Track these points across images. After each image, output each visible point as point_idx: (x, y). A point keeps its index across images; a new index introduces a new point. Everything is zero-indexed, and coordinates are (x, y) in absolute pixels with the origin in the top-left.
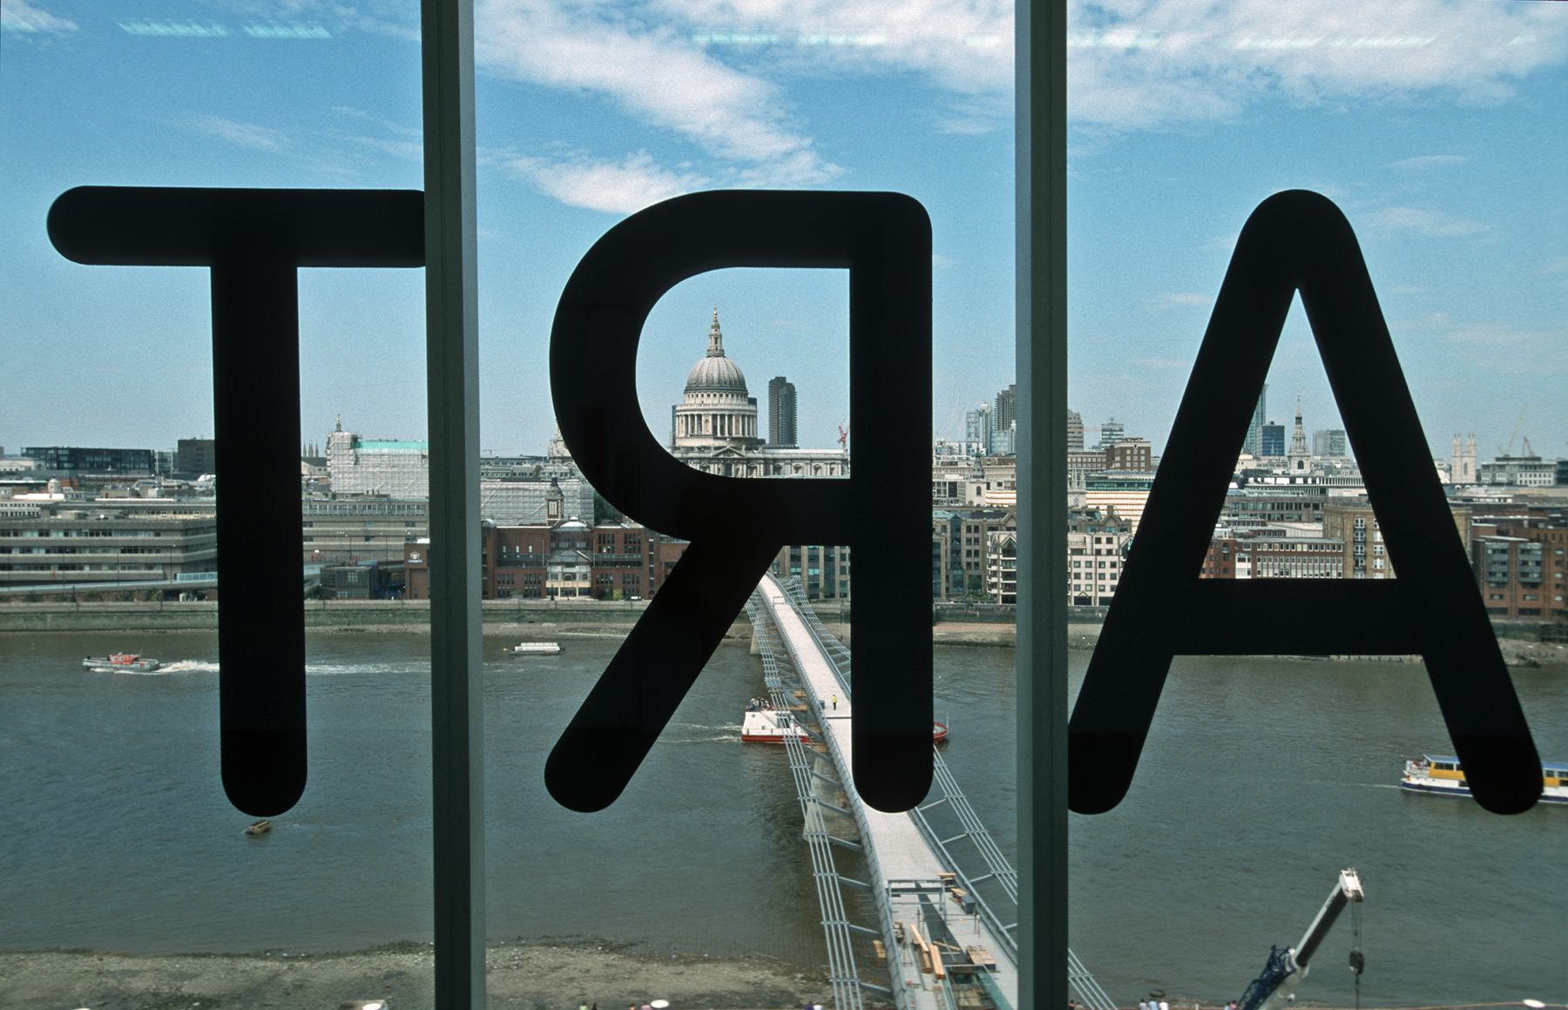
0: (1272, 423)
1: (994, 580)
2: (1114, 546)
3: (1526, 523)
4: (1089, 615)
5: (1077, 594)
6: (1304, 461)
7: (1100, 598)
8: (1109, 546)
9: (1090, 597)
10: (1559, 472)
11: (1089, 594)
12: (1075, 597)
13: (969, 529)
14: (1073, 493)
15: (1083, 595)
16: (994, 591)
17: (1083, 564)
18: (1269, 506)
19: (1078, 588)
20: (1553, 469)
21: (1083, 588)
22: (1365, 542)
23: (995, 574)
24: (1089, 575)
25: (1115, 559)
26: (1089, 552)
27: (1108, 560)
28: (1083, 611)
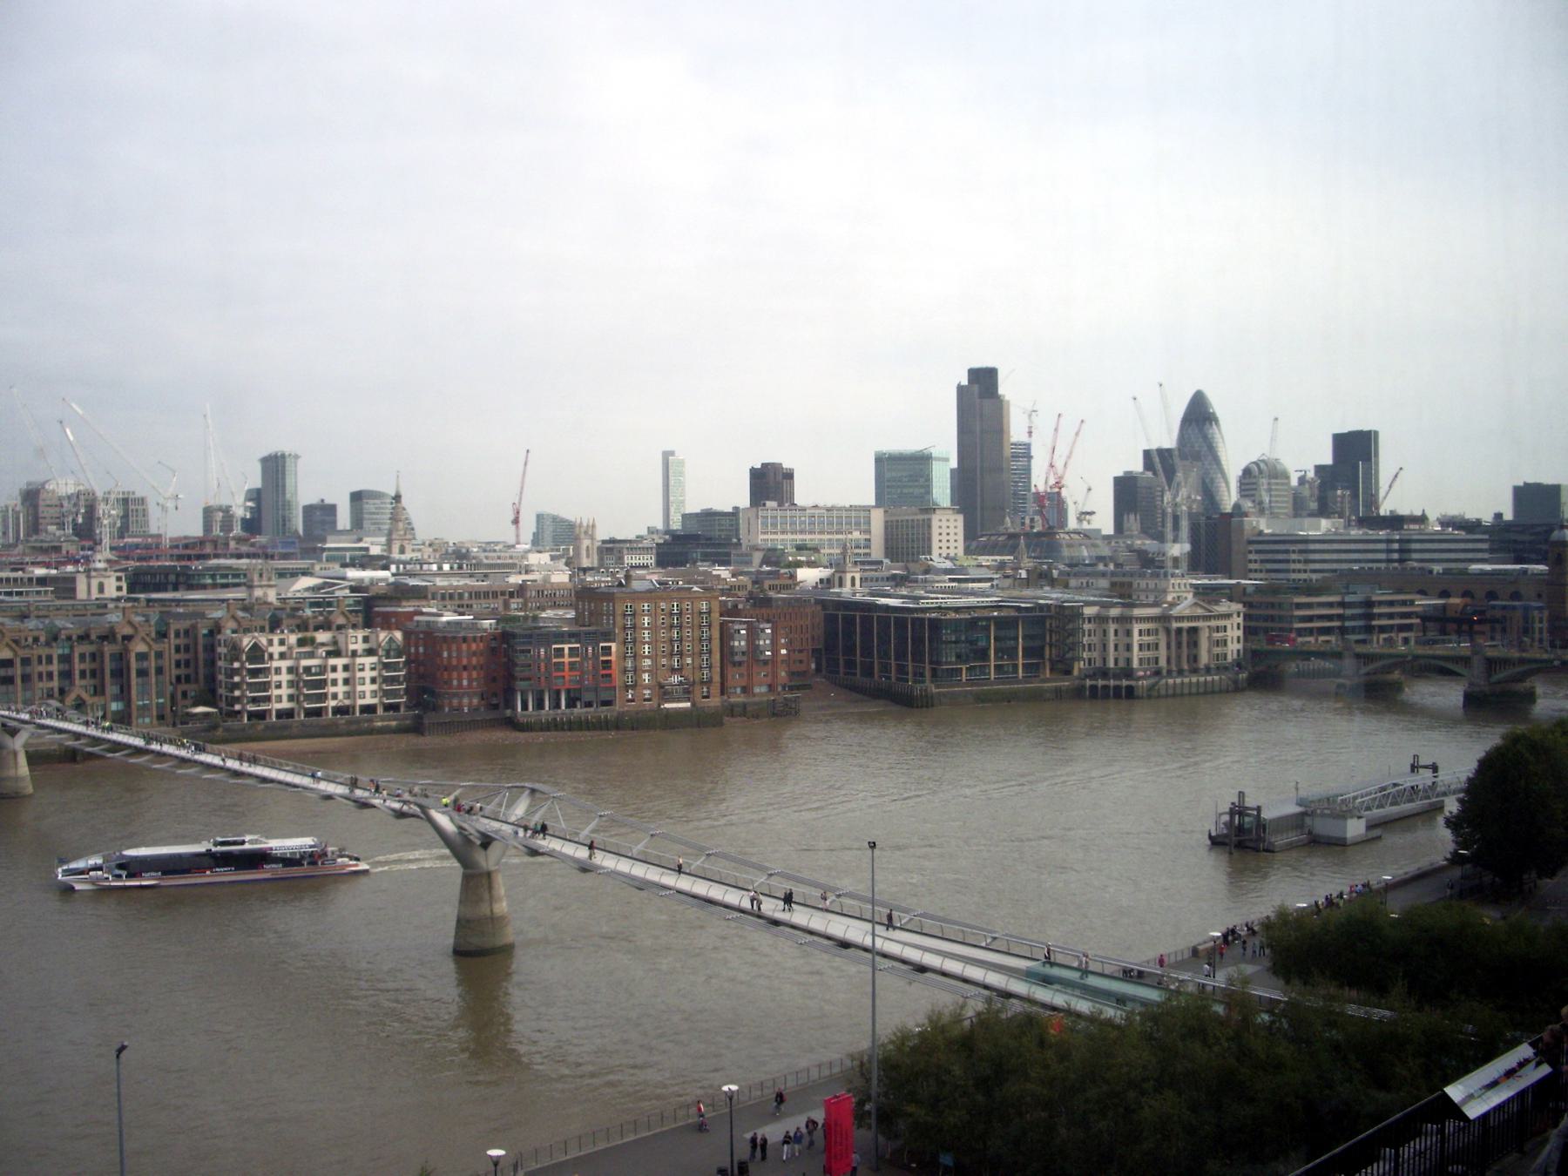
0: (323, 501)
1: (237, 693)
2: (372, 644)
3: (730, 604)
4: (354, 727)
5: (333, 703)
6: (407, 546)
7: (361, 706)
8: (366, 646)
9: (348, 707)
10: (658, 555)
11: (347, 702)
12: (333, 708)
13: (177, 635)
14: (261, 586)
15: (340, 704)
16: (237, 707)
17: (340, 668)
18: (466, 595)
19: (335, 696)
20: (654, 551)
21: (340, 696)
22: (634, 627)
23: (237, 686)
24: (346, 682)
25: (374, 659)
26: (344, 653)
27: (369, 661)
28: (349, 723)
